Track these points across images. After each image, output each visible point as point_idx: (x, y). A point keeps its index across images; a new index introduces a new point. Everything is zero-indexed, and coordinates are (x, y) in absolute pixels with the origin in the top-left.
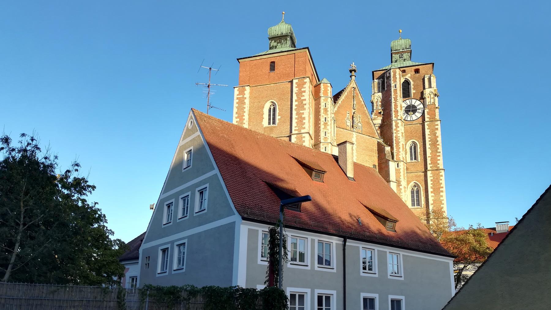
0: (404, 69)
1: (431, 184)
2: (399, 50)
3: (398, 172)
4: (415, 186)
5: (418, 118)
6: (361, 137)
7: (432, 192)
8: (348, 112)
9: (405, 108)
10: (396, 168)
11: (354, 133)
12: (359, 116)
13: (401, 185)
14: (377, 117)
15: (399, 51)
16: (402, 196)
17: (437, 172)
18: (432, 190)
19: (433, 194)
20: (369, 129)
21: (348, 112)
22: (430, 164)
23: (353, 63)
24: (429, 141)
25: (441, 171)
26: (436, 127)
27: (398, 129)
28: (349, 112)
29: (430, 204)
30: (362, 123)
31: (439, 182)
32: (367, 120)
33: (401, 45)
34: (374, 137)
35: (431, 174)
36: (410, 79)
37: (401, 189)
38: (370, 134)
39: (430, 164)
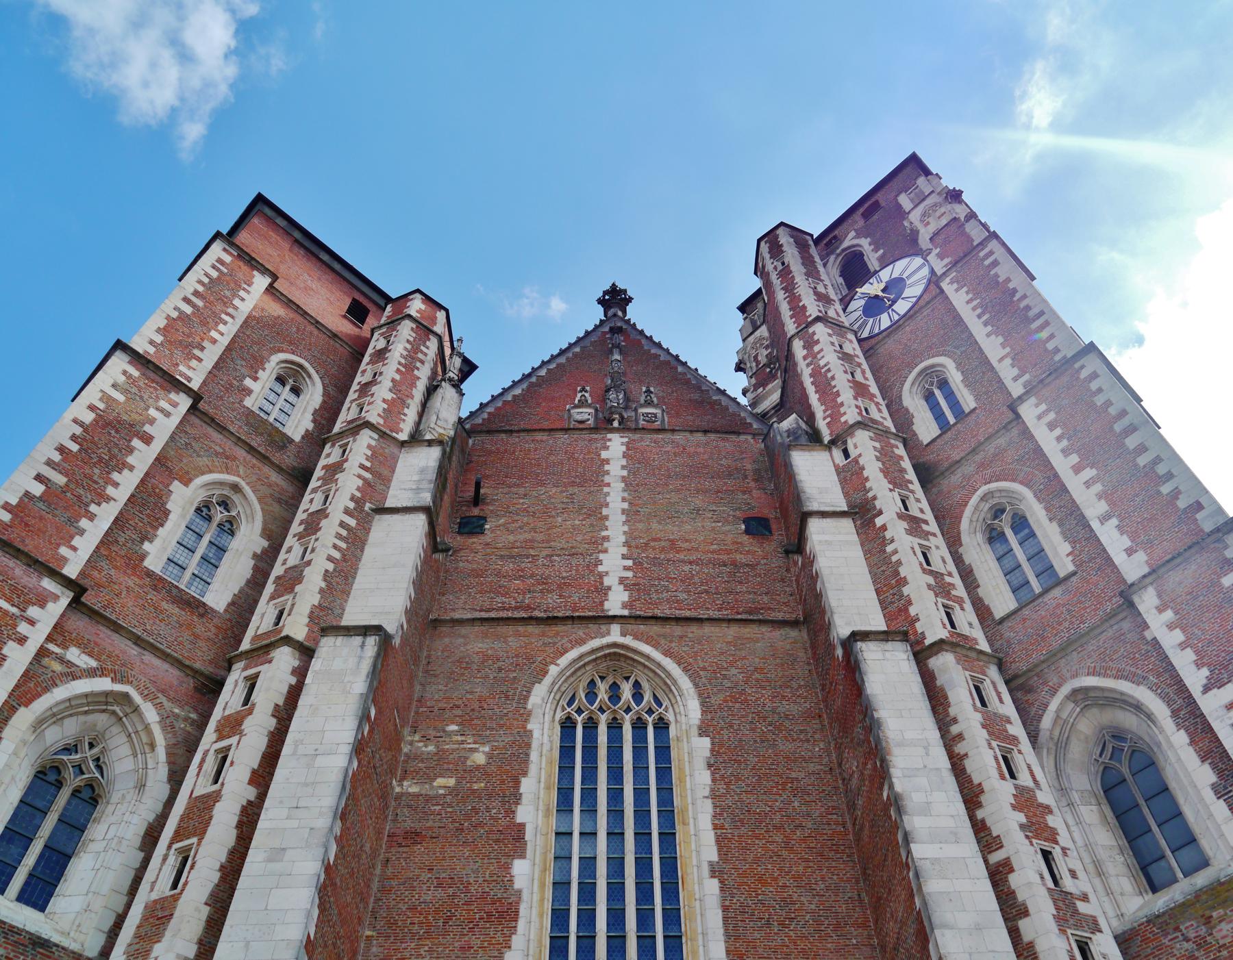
1: (1059, 439)
3: (851, 476)
4: (998, 512)
5: (914, 300)
7: (1077, 469)
10: (837, 467)
13: (880, 513)
16: (895, 552)
17: (1065, 379)
18: (1074, 459)
19: (1089, 473)
22: (1015, 379)
24: (979, 317)
25: (1077, 365)
26: (987, 262)
27: (816, 348)
29: (1095, 525)
31: (1092, 406)
34: (734, 433)
35: (1037, 406)
36: (856, 242)
37: (884, 528)
39: (1015, 379)
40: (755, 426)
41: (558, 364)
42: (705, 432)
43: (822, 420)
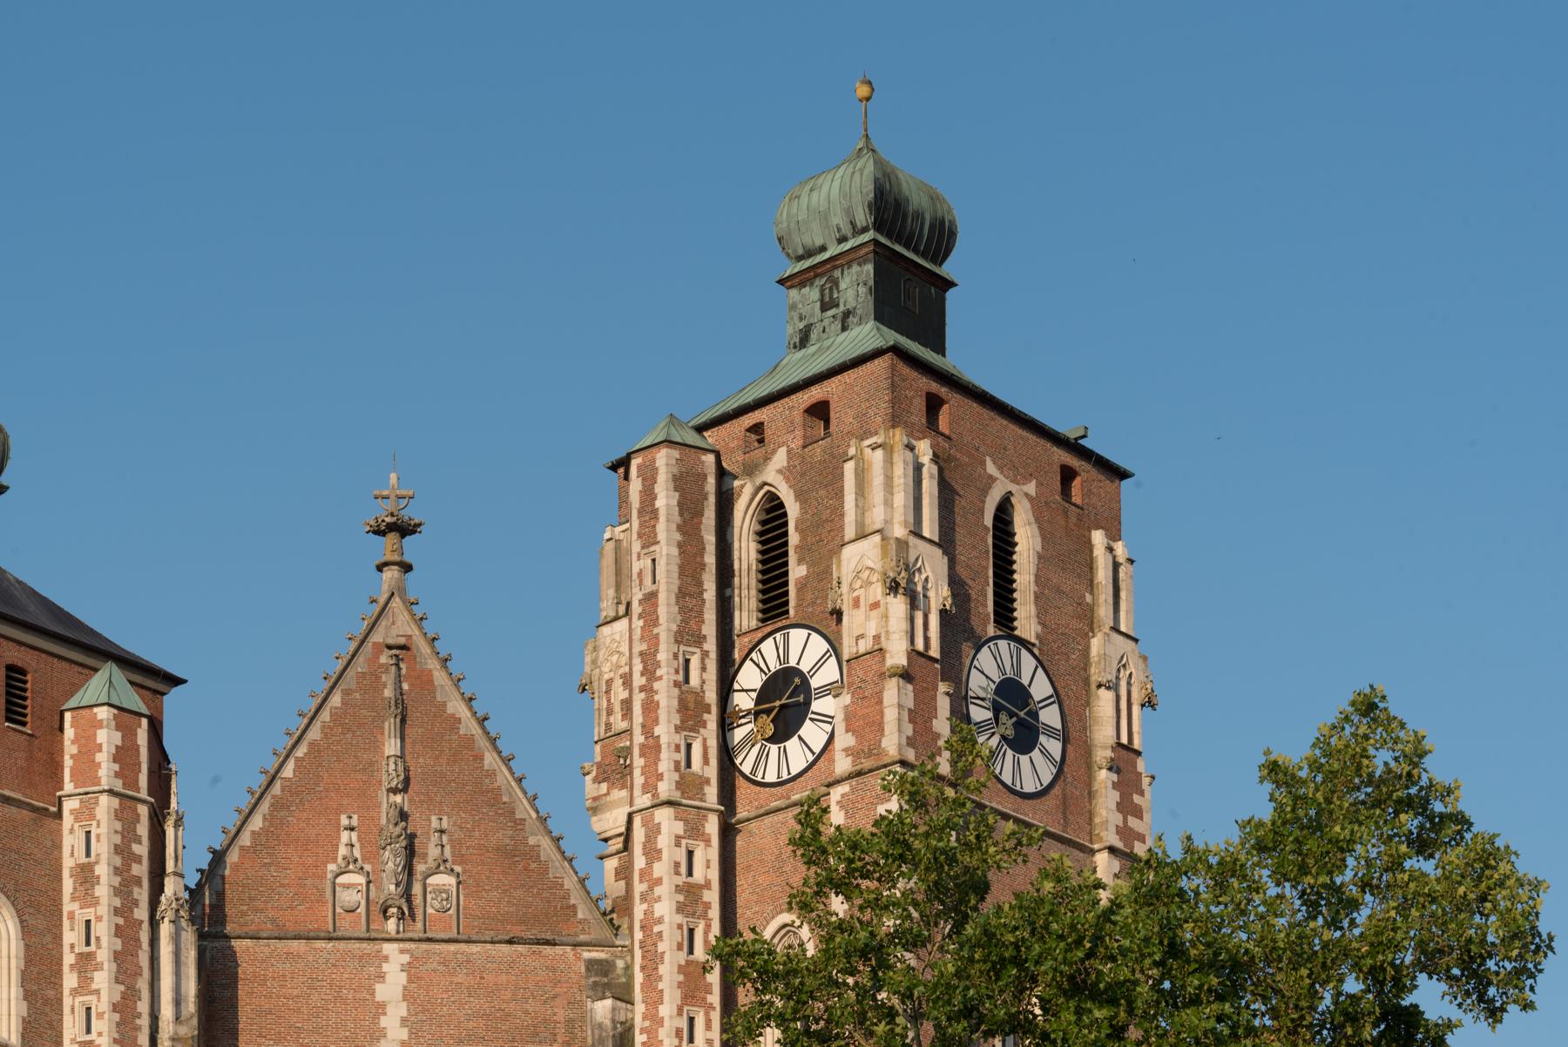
0: (815, 394)
2: (823, 249)
6: (444, 963)
8: (344, 821)
9: (754, 695)
11: (388, 948)
12: (435, 824)
14: (608, 793)
15: (826, 255)
20: (519, 893)
21: (344, 821)
23: (393, 476)
28: (355, 822)
30: (458, 869)
32: (503, 836)
33: (825, 217)
34: (548, 943)
38: (523, 922)
40: (580, 916)
41: (311, 744)
42: (510, 942)
43: (665, 935)
